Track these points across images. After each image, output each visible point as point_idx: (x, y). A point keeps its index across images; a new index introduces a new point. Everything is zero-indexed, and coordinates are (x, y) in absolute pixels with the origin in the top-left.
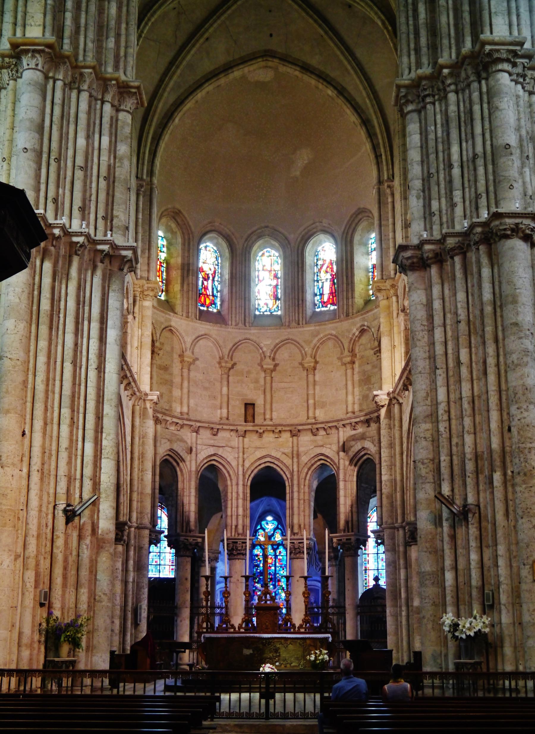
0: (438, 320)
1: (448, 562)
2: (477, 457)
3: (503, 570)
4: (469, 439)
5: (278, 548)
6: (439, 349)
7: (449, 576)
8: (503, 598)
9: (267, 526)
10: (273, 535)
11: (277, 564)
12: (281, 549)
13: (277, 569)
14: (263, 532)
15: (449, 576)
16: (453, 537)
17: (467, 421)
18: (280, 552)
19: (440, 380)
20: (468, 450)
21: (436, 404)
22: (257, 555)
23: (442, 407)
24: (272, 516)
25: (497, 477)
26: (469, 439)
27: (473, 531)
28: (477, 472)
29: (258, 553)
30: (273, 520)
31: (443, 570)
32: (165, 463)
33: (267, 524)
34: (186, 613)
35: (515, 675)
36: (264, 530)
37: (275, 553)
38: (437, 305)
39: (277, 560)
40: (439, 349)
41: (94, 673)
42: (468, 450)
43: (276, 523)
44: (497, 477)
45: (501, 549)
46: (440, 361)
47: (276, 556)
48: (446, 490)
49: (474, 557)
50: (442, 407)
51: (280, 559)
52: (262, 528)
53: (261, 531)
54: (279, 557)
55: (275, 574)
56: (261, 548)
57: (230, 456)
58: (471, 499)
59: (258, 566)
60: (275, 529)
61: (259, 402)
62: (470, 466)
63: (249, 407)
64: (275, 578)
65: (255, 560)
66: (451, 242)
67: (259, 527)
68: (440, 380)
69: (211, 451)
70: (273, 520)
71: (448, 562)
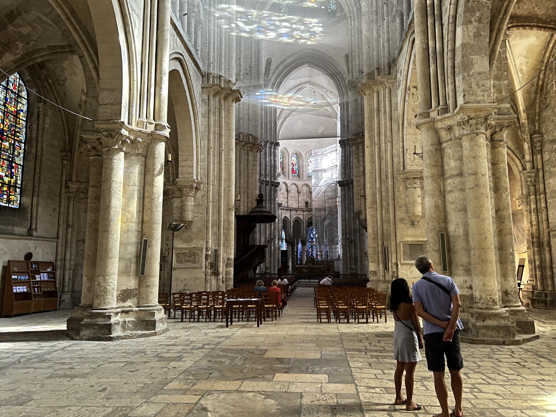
0: (347, 199)
1: (348, 252)
2: (354, 229)
3: (359, 254)
4: (352, 226)
6: (347, 205)
7: (348, 255)
8: (359, 260)
15: (348, 255)
16: (349, 246)
17: (352, 222)
19: (347, 212)
20: (352, 227)
21: (346, 217)
23: (347, 218)
25: (358, 234)
26: (352, 226)
27: (353, 245)
28: (354, 233)
31: (347, 253)
32: (284, 220)
34: (291, 260)
35: (361, 275)
38: (347, 195)
40: (347, 205)
41: (274, 274)
42: (352, 227)
44: (358, 234)
45: (358, 250)
46: (347, 208)
48: (348, 236)
49: (353, 251)
50: (347, 218)
57: (301, 217)
58: (353, 238)
60: (316, 233)
61: (309, 201)
62: (353, 232)
63: (307, 203)
66: (350, 181)
68: (347, 212)
69: (296, 216)
71: (348, 252)
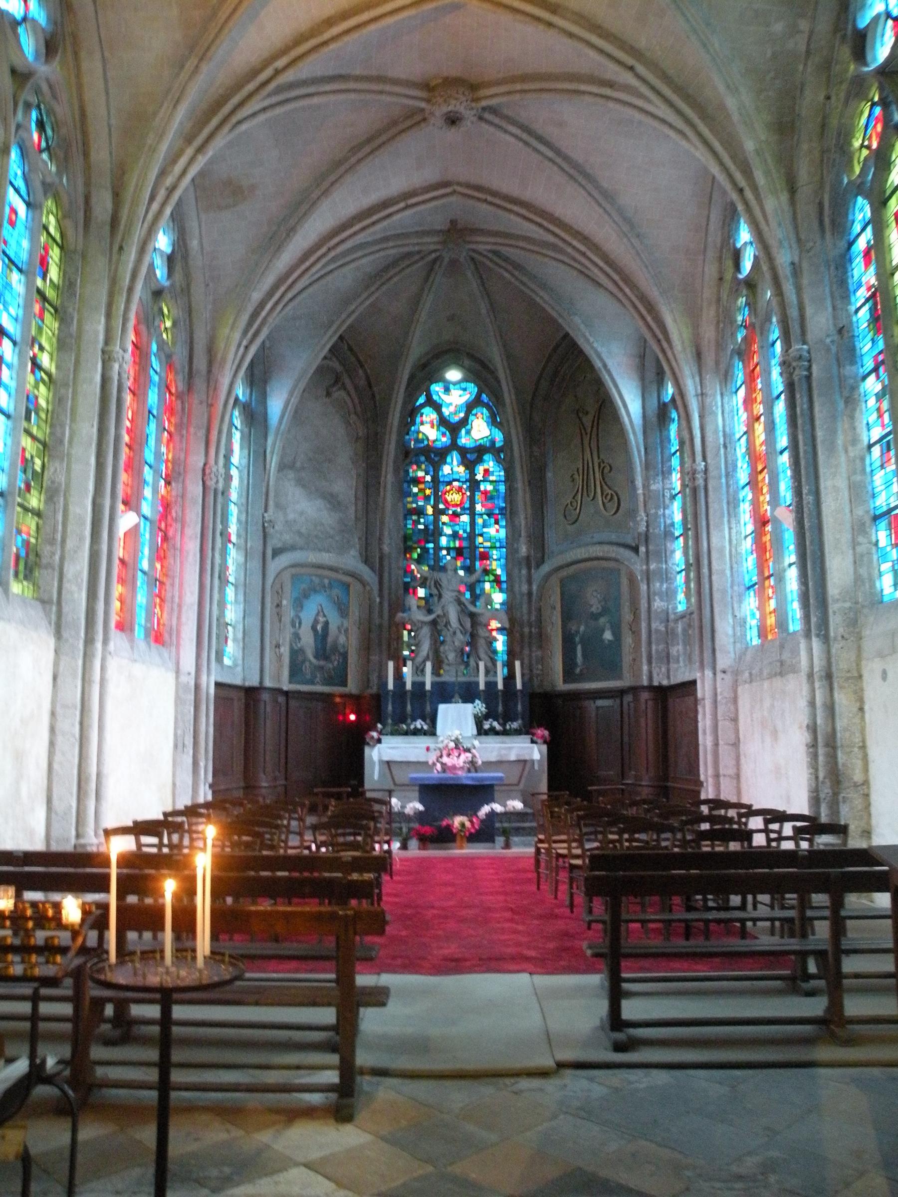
5: (479, 460)
9: (446, 398)
10: (464, 422)
11: (479, 508)
12: (489, 463)
13: (480, 521)
14: (434, 416)
18: (486, 472)
22: (417, 481)
24: (461, 366)
29: (420, 474)
30: (465, 380)
33: (447, 390)
36: (437, 407)
37: (473, 474)
39: (478, 496)
43: (473, 388)
47: (474, 484)
51: (485, 493)
52: (430, 402)
53: (429, 414)
54: (482, 488)
55: (472, 536)
56: (428, 459)
59: (420, 512)
60: (470, 407)
64: (473, 547)
65: (409, 493)
67: (422, 400)
70: (465, 380)
